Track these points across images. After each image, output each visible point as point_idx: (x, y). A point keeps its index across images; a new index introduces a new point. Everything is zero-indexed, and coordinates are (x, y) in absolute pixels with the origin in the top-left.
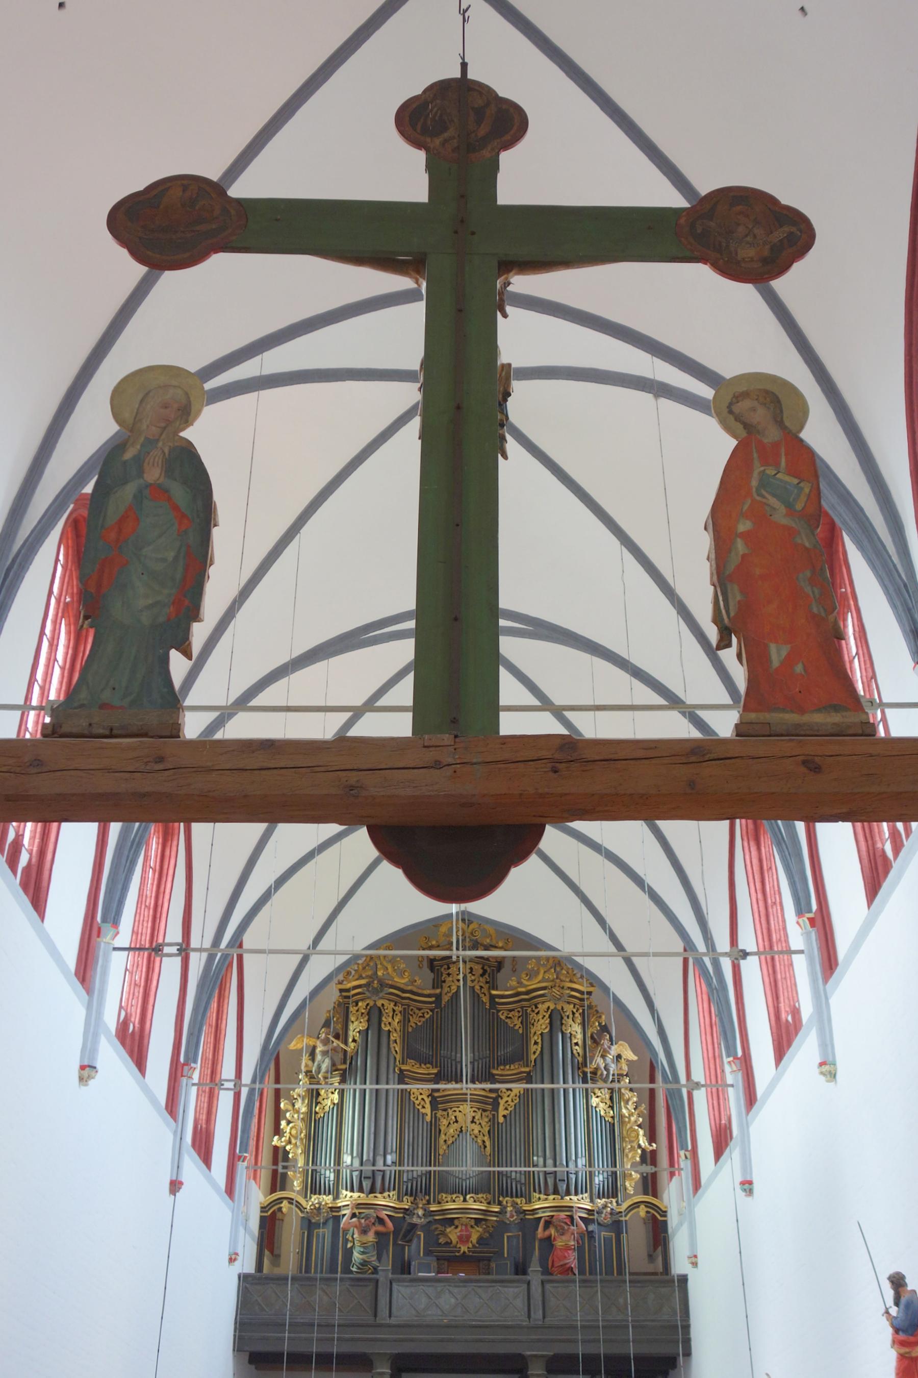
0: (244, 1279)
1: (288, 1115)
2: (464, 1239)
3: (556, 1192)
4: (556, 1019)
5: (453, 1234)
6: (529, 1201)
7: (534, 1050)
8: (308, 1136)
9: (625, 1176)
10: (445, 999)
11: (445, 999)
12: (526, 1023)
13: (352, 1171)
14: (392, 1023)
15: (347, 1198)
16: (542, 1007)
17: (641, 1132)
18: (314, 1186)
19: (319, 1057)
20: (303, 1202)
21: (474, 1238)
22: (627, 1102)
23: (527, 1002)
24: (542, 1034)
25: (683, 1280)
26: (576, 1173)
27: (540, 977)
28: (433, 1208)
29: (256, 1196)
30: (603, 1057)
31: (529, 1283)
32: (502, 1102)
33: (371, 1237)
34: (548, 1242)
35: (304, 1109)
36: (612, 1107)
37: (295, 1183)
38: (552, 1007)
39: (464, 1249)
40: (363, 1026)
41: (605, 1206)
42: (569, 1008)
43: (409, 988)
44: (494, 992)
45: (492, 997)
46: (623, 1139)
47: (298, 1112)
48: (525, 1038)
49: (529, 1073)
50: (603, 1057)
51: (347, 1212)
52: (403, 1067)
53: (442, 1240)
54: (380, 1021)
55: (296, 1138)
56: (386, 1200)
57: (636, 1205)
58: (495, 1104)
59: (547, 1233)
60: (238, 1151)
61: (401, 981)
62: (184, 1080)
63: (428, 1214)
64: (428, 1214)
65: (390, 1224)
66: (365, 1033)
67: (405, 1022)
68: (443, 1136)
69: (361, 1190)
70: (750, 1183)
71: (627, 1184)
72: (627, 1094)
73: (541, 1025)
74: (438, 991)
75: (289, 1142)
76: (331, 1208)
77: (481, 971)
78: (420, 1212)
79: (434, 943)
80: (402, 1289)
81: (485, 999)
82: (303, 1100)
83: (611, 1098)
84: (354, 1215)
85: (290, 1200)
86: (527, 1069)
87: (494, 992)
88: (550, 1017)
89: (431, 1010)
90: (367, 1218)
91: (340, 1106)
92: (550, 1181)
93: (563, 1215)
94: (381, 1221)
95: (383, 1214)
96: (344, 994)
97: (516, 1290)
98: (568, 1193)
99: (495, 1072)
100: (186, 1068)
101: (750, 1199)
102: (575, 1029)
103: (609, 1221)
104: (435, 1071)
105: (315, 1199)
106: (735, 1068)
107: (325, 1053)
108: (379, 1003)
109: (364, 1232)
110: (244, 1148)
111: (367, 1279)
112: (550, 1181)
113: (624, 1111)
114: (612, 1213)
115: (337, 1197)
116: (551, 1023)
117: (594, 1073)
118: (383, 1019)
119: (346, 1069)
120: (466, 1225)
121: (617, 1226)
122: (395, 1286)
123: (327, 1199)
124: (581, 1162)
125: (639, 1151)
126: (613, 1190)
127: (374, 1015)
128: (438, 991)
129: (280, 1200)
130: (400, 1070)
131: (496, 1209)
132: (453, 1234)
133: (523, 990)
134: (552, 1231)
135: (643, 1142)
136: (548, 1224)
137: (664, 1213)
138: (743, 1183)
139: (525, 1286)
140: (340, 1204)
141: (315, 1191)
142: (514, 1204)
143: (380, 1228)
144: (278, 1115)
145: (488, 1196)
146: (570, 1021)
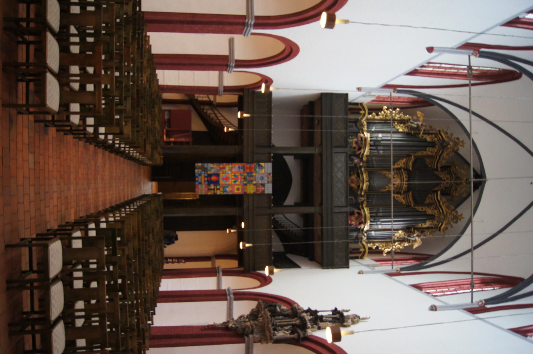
0: (346, 95)
1: (394, 112)
2: (352, 181)
3: (371, 217)
4: (431, 217)
5: (354, 177)
6: (367, 206)
7: (419, 208)
8: (386, 120)
9: (374, 243)
10: (436, 173)
11: (436, 173)
12: (429, 205)
13: (377, 137)
14: (429, 151)
15: (367, 135)
16: (436, 211)
17: (389, 250)
18: (370, 123)
19: (416, 123)
20: (364, 119)
21: (353, 185)
22: (400, 244)
23: (436, 205)
24: (425, 211)
25: (347, 266)
26: (377, 225)
27: (448, 211)
28: (363, 169)
29: (366, 100)
30: (417, 236)
31: (346, 207)
32: (399, 196)
33: (354, 145)
34: (352, 214)
35: (396, 118)
36: (398, 238)
37: (370, 116)
38: (436, 215)
39: (349, 181)
40: (428, 139)
41: (364, 236)
42: (435, 222)
43: (441, 158)
44: (439, 192)
45: (437, 192)
46: (386, 242)
47: (395, 116)
48: (423, 204)
49: (411, 206)
50: (417, 236)
51: (362, 135)
52: (413, 157)
53: (352, 173)
54: (430, 147)
55: (386, 116)
56: (367, 151)
57: (364, 247)
58: (399, 193)
59: (356, 213)
60: (398, 89)
61: (444, 155)
62: (472, 51)
63: (361, 167)
64: (361, 167)
65: (359, 152)
66: (425, 141)
67: (429, 157)
68: (387, 173)
69: (371, 141)
70: (436, 310)
71: (371, 244)
72: (402, 245)
73: (429, 211)
74: (439, 169)
75: (385, 112)
76: (363, 130)
77: (446, 186)
78: (361, 164)
79: (457, 168)
80: (343, 157)
81: (436, 189)
82: (400, 117)
83: (401, 238)
84: (362, 138)
85: (364, 114)
86: (412, 205)
87: (439, 192)
88: (432, 215)
89: (431, 167)
90: (362, 143)
91: (397, 132)
92: (374, 214)
93: (363, 220)
94: (360, 149)
95: (362, 151)
96: (438, 132)
97: (344, 202)
98: (371, 221)
99: (410, 193)
100: (477, 52)
101: (428, 309)
102: (428, 224)
103: (359, 237)
104: (410, 169)
105: (365, 123)
106: (480, 303)
107: (418, 125)
108: (437, 146)
109: (356, 143)
110: (399, 92)
111: (346, 144)
112: (374, 214)
113: (397, 243)
114: (362, 238)
115: (368, 132)
116: (430, 215)
117: (411, 232)
118: (431, 148)
119: (412, 134)
120: (358, 181)
121: (358, 240)
122: (344, 154)
123: (365, 128)
124: (380, 227)
125: (383, 249)
126: (369, 238)
127: (432, 144)
128: (439, 169)
129: (365, 110)
130: (411, 156)
131: (363, 193)
132: (354, 177)
133: (441, 203)
134: (356, 215)
135: (387, 250)
136: (359, 214)
137: (362, 258)
138: (435, 306)
139: (345, 205)
140: (365, 133)
141: (368, 123)
142: (364, 200)
143: (357, 149)
144: (394, 109)
145: (367, 191)
146: (430, 223)
